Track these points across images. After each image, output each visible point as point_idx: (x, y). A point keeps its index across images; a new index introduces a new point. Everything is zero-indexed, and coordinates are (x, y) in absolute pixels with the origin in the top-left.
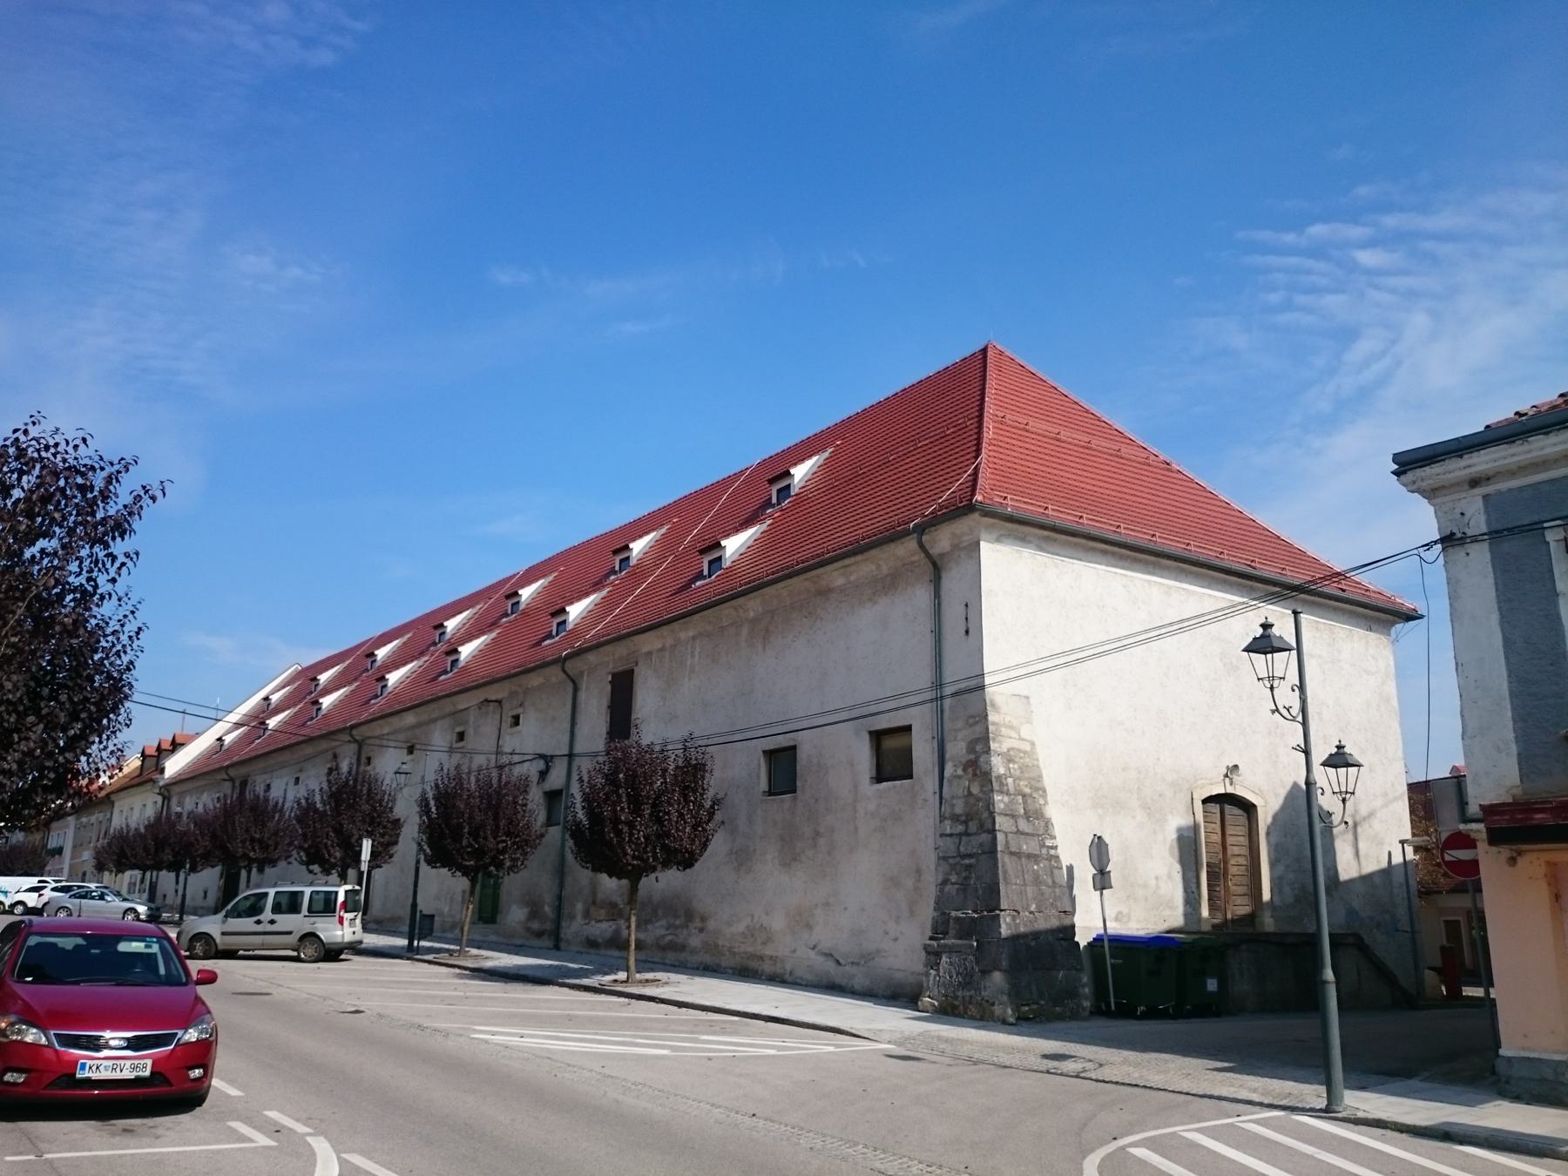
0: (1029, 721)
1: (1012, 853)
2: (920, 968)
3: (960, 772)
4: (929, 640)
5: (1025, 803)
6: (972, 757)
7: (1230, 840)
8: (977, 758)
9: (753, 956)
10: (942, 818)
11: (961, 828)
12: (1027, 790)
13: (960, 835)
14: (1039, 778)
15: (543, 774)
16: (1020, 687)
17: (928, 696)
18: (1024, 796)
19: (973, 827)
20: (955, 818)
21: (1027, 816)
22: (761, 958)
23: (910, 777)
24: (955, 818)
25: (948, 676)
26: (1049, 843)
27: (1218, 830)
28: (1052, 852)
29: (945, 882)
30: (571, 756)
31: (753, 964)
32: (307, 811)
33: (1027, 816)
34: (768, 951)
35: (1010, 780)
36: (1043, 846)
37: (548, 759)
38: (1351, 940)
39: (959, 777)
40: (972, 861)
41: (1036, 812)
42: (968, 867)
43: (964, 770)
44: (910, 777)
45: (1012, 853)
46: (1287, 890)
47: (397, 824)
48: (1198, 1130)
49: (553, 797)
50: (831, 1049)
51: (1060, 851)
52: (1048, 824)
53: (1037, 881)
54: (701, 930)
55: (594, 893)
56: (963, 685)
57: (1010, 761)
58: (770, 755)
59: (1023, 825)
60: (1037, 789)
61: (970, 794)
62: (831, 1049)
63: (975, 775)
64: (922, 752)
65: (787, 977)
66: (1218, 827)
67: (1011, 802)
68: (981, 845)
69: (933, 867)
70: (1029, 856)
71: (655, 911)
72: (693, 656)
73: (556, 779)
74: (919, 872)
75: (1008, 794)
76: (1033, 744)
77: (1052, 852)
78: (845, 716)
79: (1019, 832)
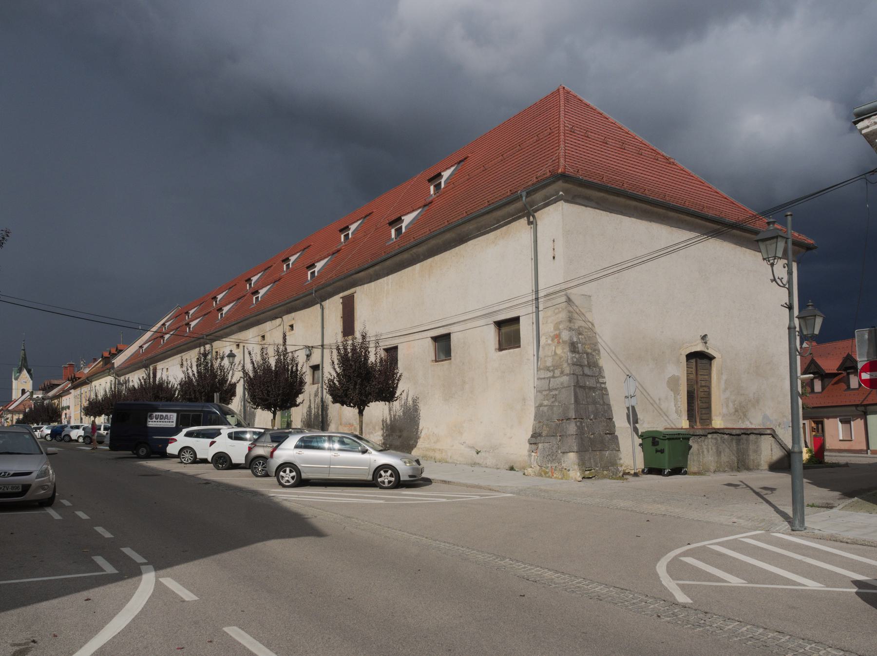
0: (590, 311)
1: (581, 387)
2: (526, 453)
3: (550, 342)
4: (531, 265)
5: (588, 358)
6: (557, 332)
7: (700, 377)
8: (560, 334)
9: (428, 449)
10: (538, 369)
11: (550, 374)
12: (589, 351)
13: (549, 378)
14: (596, 344)
15: (308, 356)
16: (585, 290)
17: (530, 298)
18: (587, 354)
19: (557, 373)
20: (547, 369)
21: (589, 365)
22: (434, 450)
23: (519, 347)
24: (547, 369)
25: (541, 286)
26: (601, 380)
27: (694, 372)
28: (603, 386)
29: (541, 405)
30: (322, 346)
31: (431, 454)
32: (186, 385)
33: (589, 365)
34: (438, 446)
35: (579, 345)
36: (598, 382)
37: (310, 348)
38: (769, 432)
39: (549, 345)
40: (557, 392)
41: (594, 363)
42: (555, 396)
43: (552, 340)
44: (519, 347)
45: (581, 387)
46: (731, 405)
47: (233, 386)
48: (718, 544)
49: (315, 368)
50: (478, 497)
51: (607, 385)
52: (601, 369)
53: (594, 403)
54: (400, 437)
55: (340, 419)
56: (551, 290)
57: (580, 334)
58: (435, 339)
59: (587, 371)
60: (595, 350)
61: (555, 354)
62: (478, 497)
63: (559, 342)
64: (526, 329)
65: (449, 460)
66: (694, 370)
67: (580, 357)
68: (562, 384)
69: (532, 397)
70: (590, 388)
71: (374, 428)
72: (388, 285)
73: (315, 359)
74: (524, 399)
75: (578, 353)
76: (593, 325)
77: (603, 386)
78: (479, 314)
79: (584, 375)
